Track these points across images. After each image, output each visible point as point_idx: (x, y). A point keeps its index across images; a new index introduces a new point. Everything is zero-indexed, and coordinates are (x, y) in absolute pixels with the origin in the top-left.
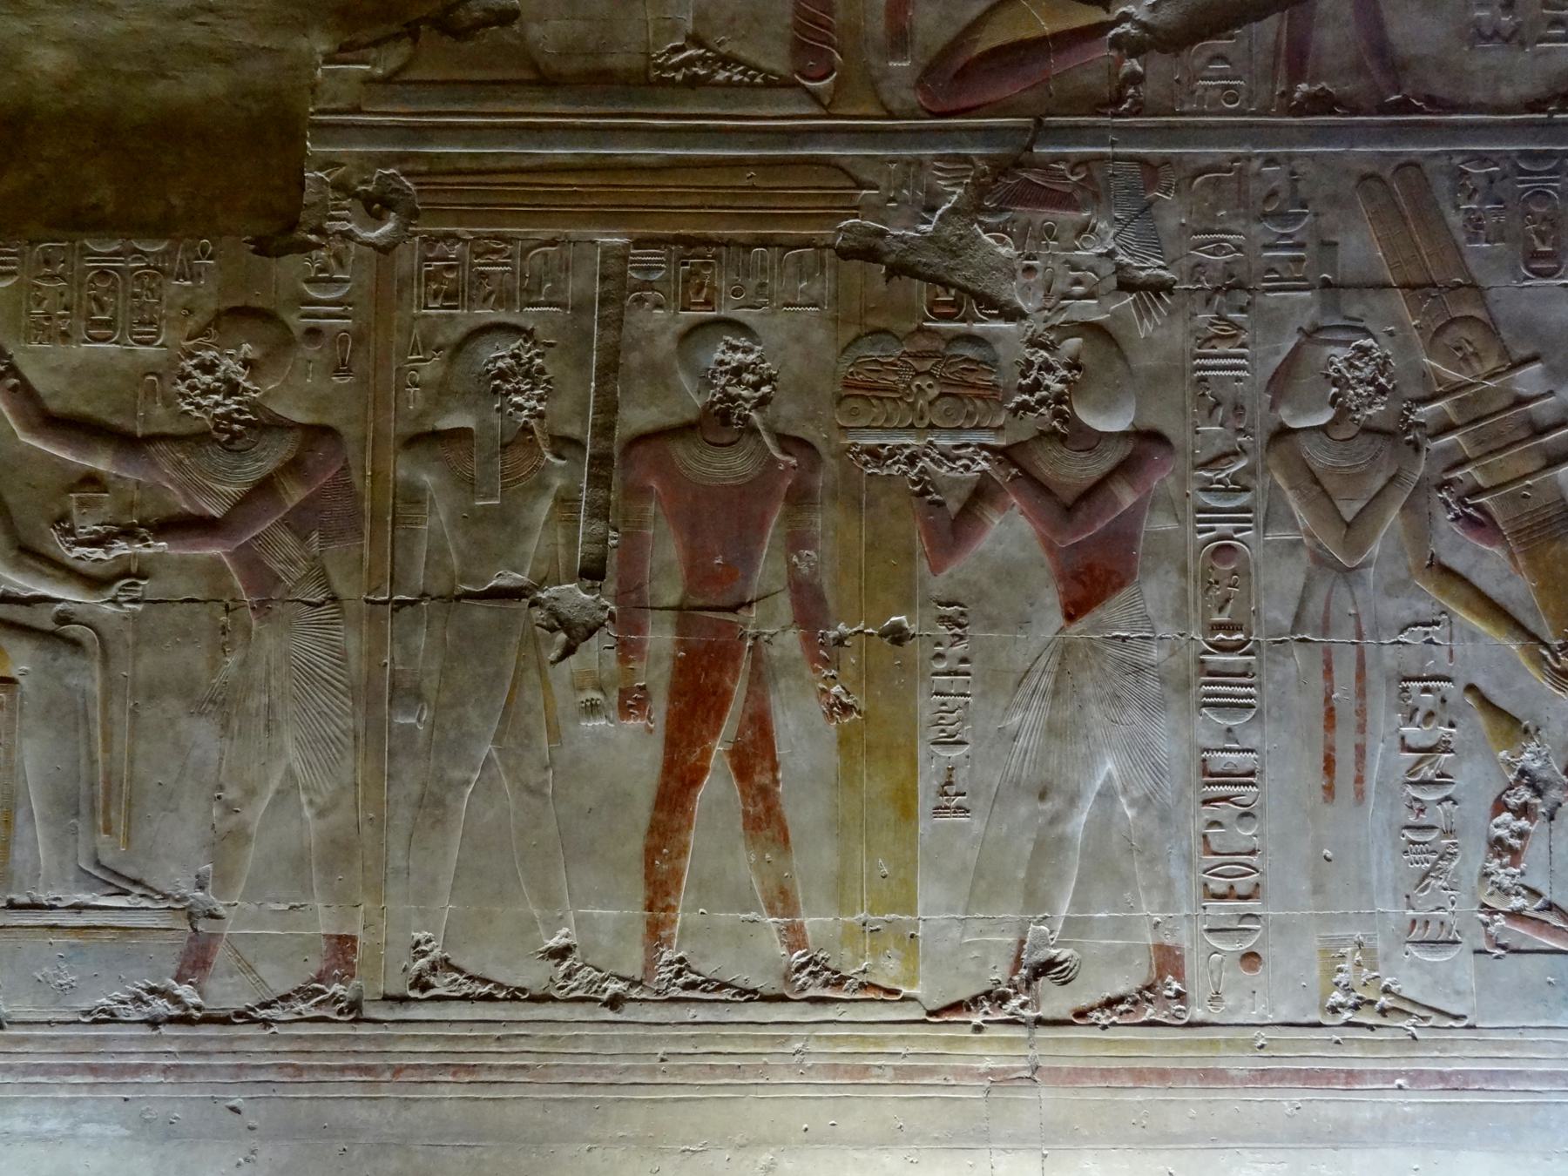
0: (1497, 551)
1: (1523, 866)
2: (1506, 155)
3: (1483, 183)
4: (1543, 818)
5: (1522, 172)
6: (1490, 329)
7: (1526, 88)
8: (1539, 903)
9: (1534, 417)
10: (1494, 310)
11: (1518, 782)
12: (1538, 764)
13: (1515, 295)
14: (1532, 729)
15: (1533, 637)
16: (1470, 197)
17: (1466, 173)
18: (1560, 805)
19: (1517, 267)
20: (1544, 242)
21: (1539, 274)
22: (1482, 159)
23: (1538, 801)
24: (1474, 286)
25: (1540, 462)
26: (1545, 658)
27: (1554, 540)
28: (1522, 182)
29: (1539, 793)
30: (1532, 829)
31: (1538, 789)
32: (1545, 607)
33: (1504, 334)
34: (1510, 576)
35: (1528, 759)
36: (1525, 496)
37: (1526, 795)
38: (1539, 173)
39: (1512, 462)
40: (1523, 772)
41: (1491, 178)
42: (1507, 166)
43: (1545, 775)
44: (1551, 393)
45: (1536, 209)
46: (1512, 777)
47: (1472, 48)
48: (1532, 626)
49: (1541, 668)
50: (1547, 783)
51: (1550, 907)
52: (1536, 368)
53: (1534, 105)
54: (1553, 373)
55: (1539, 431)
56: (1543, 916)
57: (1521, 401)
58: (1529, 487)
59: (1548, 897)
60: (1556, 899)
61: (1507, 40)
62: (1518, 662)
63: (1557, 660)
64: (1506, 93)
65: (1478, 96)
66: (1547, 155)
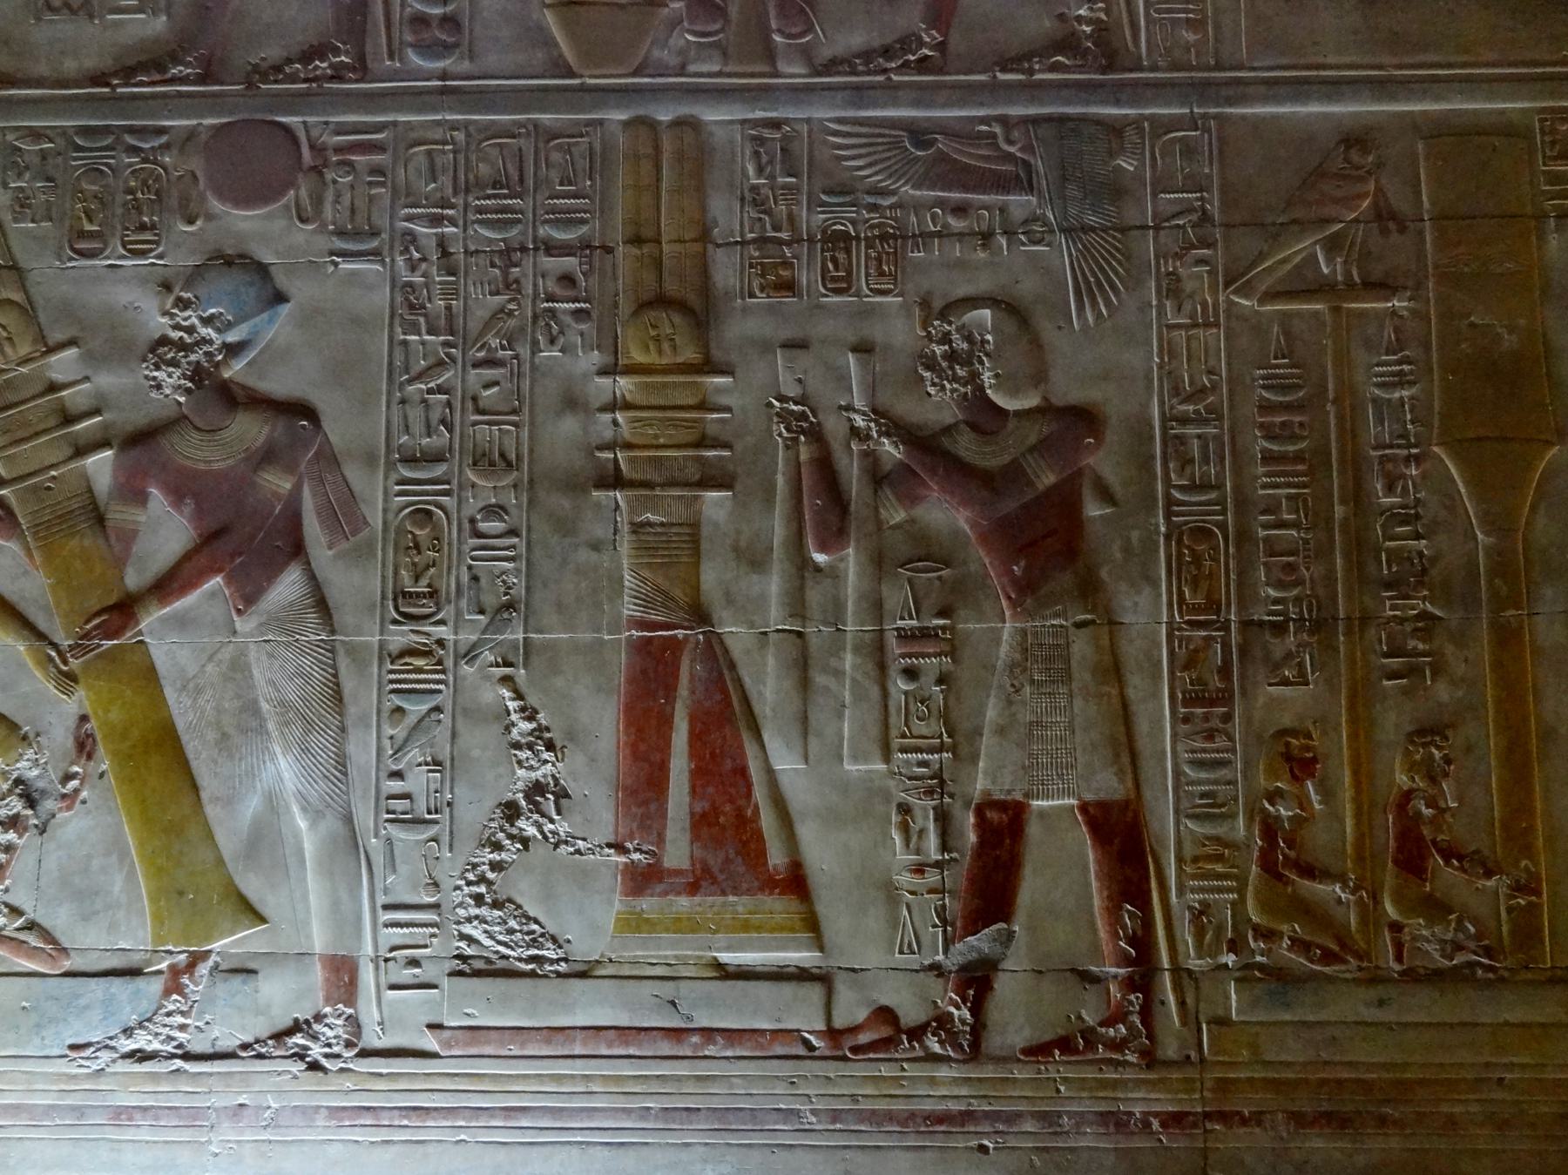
0: (13, 546)
1: (7, 882)
2: (63, 132)
3: (37, 160)
4: (35, 831)
5: (79, 149)
6: (28, 311)
7: (91, 63)
8: (20, 922)
9: (68, 404)
10: (32, 291)
11: (10, 792)
12: (35, 772)
13: (55, 276)
14: (31, 736)
15: (41, 636)
16: (20, 175)
17: (20, 149)
18: (54, 816)
19: (61, 248)
20: (91, 221)
21: (82, 254)
22: (36, 135)
23: (30, 812)
24: (15, 268)
25: (69, 451)
26: (51, 659)
27: (73, 535)
28: (75, 159)
29: (31, 803)
30: (20, 842)
31: (31, 801)
32: (58, 604)
33: (42, 318)
34: (26, 573)
35: (25, 767)
36: (49, 488)
37: (16, 805)
38: (91, 150)
39: (43, 450)
40: (18, 781)
41: (44, 155)
42: (61, 142)
43: (41, 784)
44: (87, 379)
45: (85, 186)
46: (5, 787)
47: (39, 19)
48: (42, 624)
49: (45, 670)
50: (43, 792)
51: (31, 926)
52: (71, 352)
53: (99, 79)
54: (90, 358)
55: (68, 419)
56: (22, 936)
57: (53, 387)
58: (54, 477)
59: (32, 916)
60: (39, 920)
61: (73, 12)
62: (25, 665)
63: (65, 662)
64: (70, 66)
65: (43, 69)
66: (107, 130)
